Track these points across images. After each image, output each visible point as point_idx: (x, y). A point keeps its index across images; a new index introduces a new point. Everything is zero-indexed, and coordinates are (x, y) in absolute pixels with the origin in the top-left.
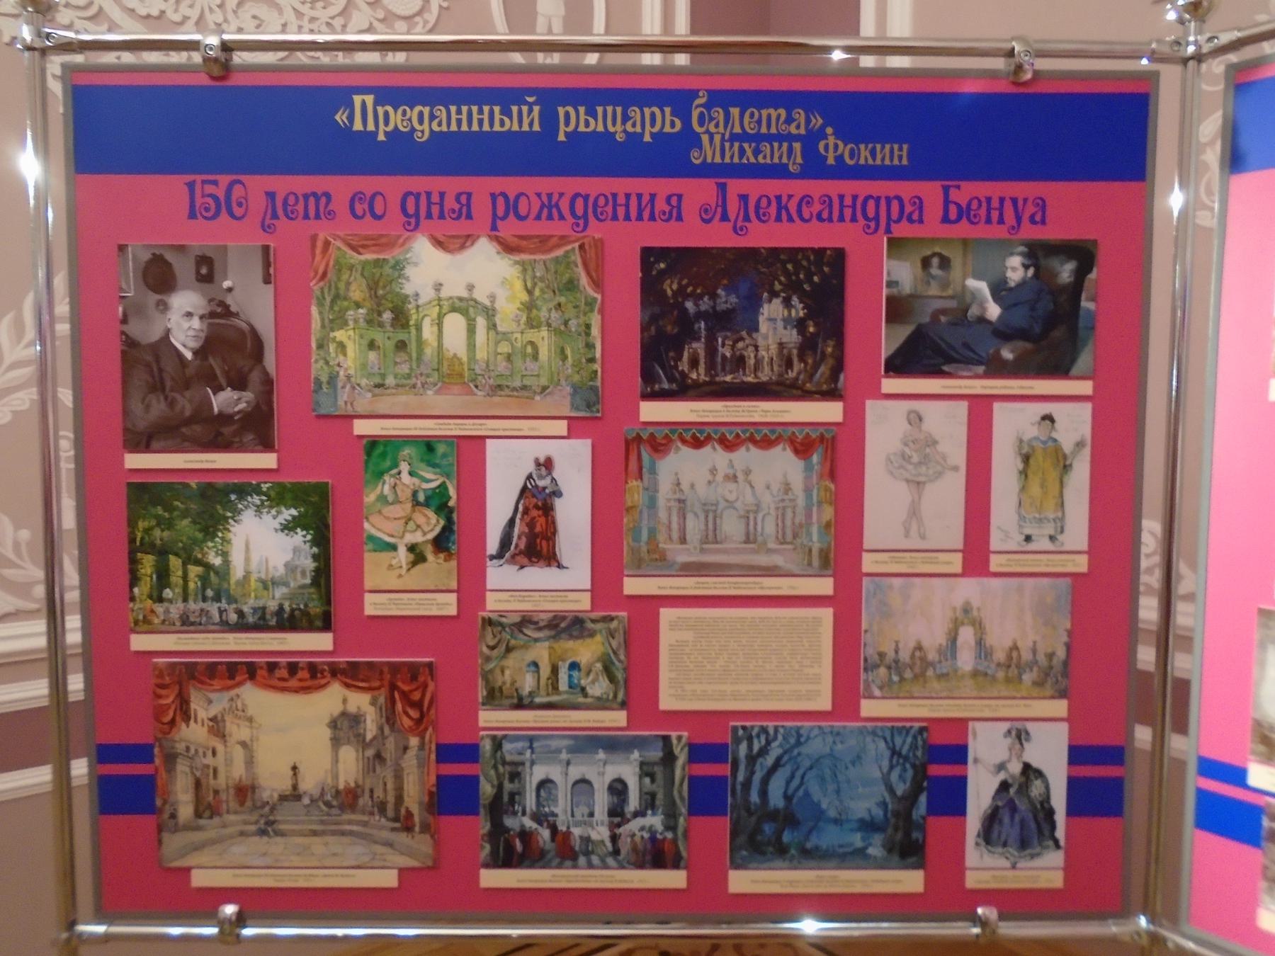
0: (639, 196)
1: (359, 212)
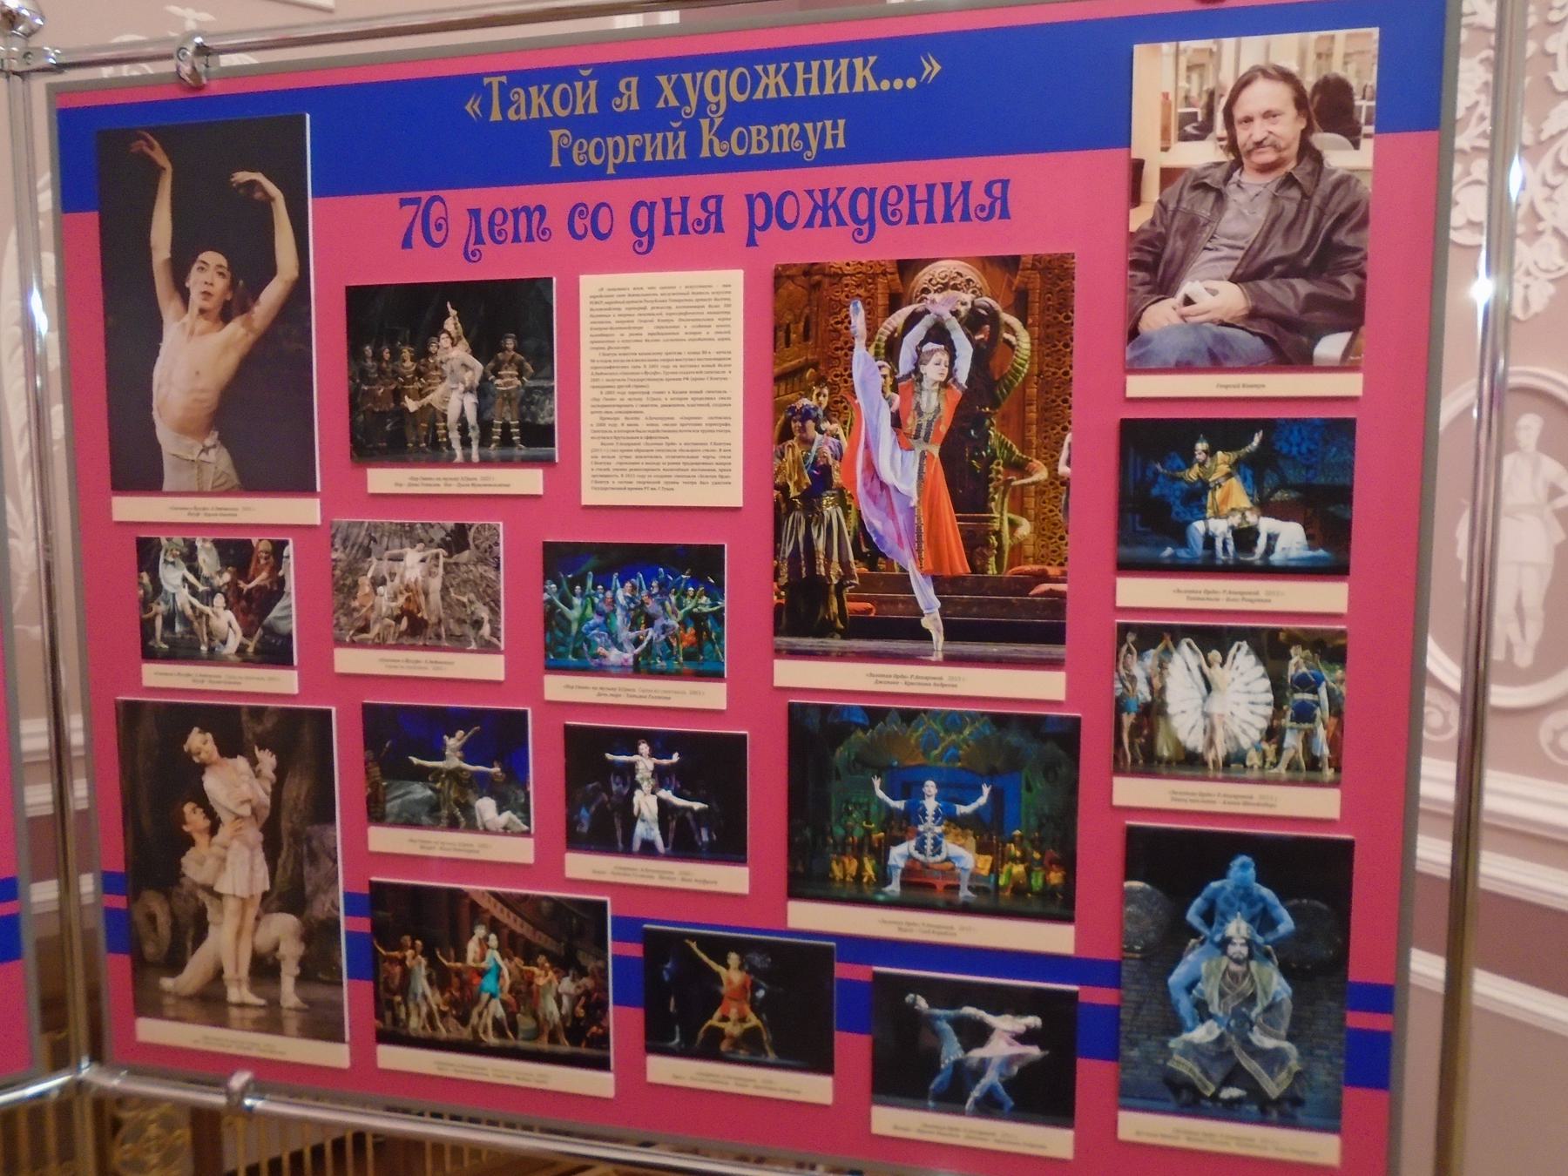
0: (947, 187)
1: (580, 231)
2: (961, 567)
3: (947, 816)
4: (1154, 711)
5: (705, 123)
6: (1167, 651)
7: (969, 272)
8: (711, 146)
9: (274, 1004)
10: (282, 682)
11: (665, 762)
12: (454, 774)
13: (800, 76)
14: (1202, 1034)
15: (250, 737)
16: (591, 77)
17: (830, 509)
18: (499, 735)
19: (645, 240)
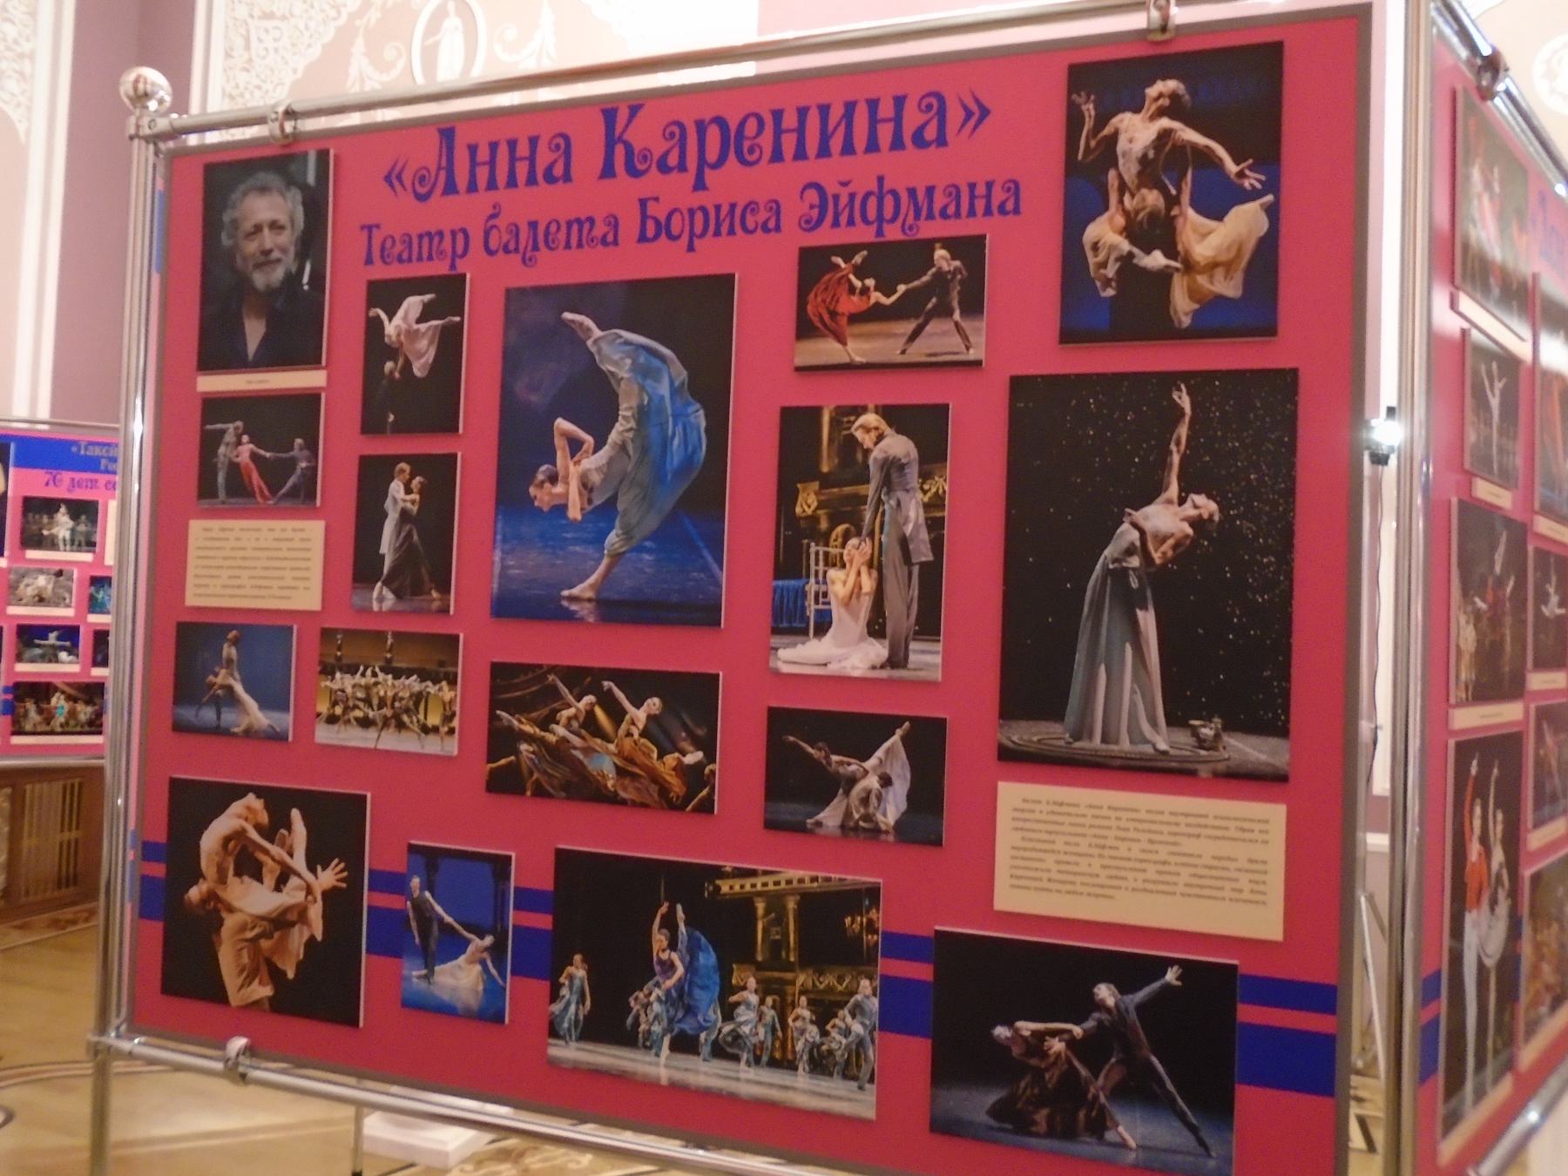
12: (52, 646)
18: (69, 634)
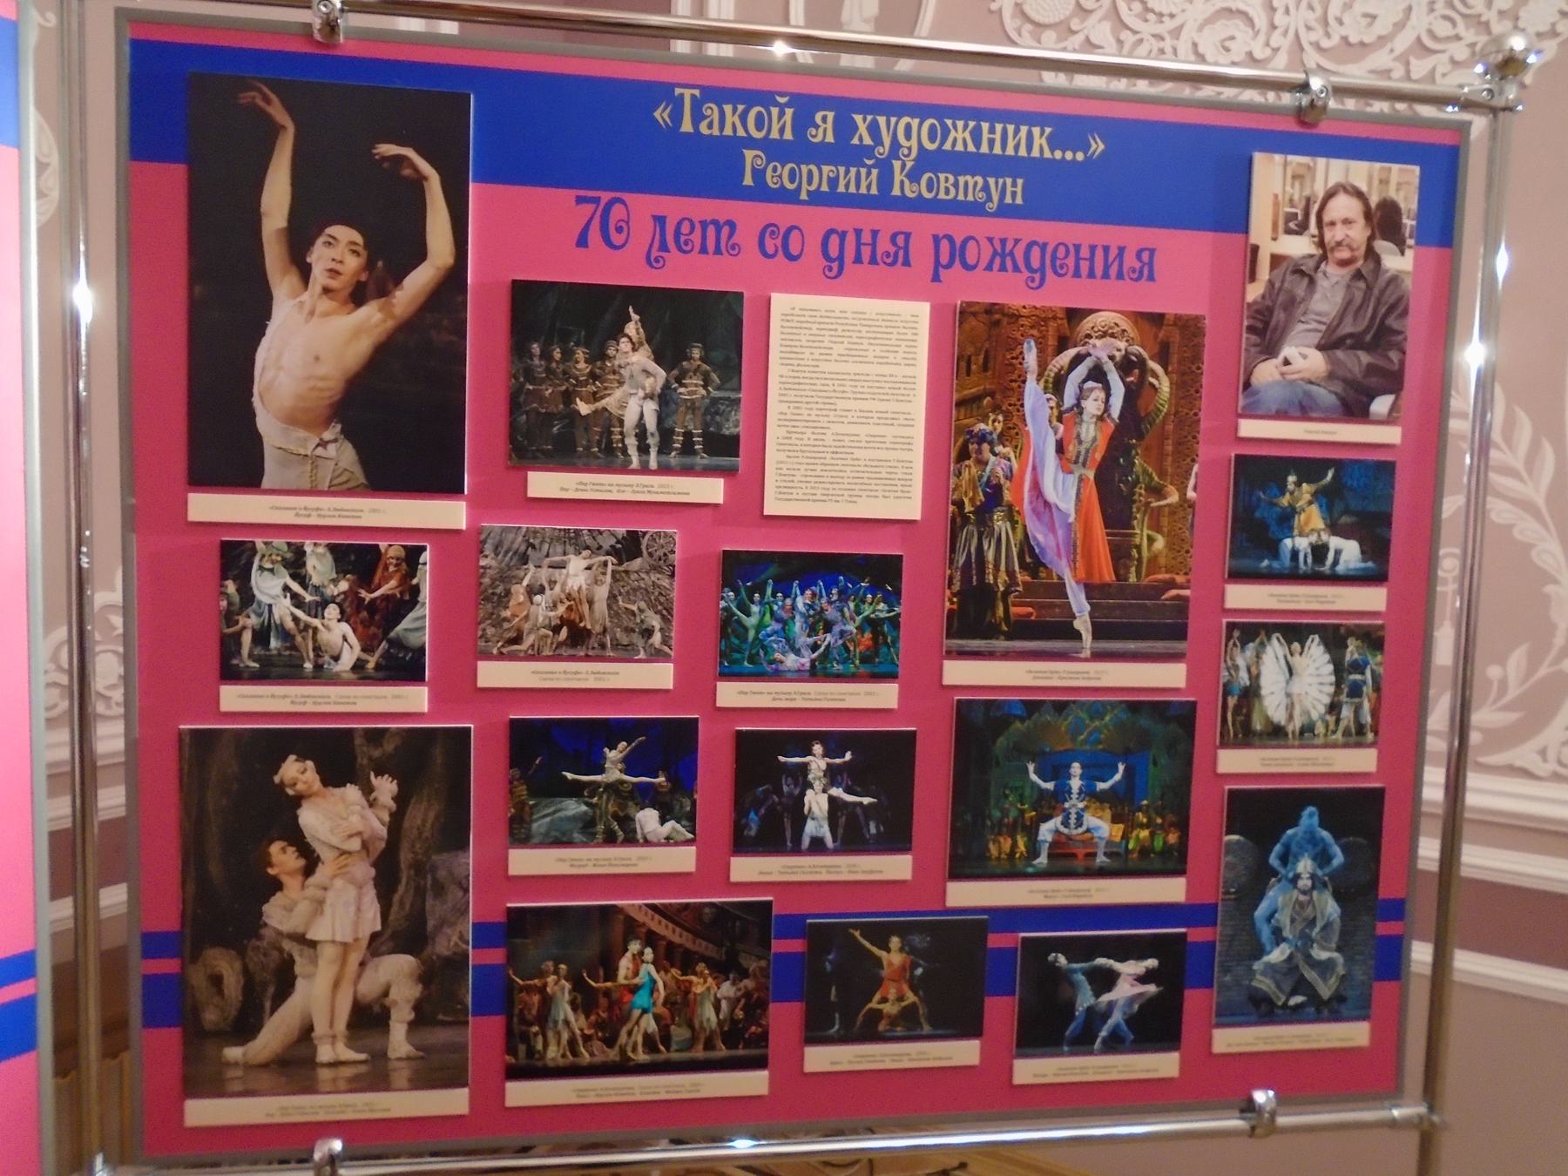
0: (1106, 249)
1: (770, 250)
2: (1109, 576)
3: (1089, 793)
4: (1251, 694)
5: (897, 164)
6: (1262, 645)
7: (1125, 324)
8: (901, 185)
9: (379, 1057)
10: (414, 699)
11: (838, 761)
12: (613, 788)
13: (985, 135)
14: (1277, 955)
15: (365, 762)
16: (788, 105)
17: (1000, 524)
18: (665, 748)
19: (835, 265)
